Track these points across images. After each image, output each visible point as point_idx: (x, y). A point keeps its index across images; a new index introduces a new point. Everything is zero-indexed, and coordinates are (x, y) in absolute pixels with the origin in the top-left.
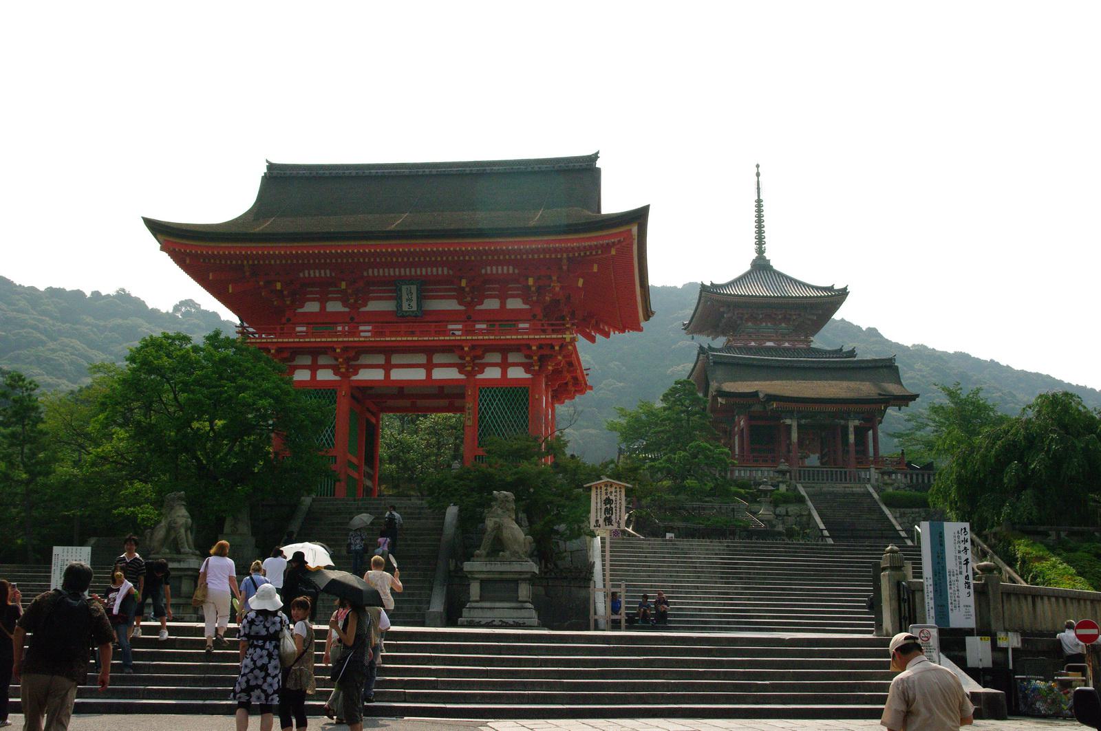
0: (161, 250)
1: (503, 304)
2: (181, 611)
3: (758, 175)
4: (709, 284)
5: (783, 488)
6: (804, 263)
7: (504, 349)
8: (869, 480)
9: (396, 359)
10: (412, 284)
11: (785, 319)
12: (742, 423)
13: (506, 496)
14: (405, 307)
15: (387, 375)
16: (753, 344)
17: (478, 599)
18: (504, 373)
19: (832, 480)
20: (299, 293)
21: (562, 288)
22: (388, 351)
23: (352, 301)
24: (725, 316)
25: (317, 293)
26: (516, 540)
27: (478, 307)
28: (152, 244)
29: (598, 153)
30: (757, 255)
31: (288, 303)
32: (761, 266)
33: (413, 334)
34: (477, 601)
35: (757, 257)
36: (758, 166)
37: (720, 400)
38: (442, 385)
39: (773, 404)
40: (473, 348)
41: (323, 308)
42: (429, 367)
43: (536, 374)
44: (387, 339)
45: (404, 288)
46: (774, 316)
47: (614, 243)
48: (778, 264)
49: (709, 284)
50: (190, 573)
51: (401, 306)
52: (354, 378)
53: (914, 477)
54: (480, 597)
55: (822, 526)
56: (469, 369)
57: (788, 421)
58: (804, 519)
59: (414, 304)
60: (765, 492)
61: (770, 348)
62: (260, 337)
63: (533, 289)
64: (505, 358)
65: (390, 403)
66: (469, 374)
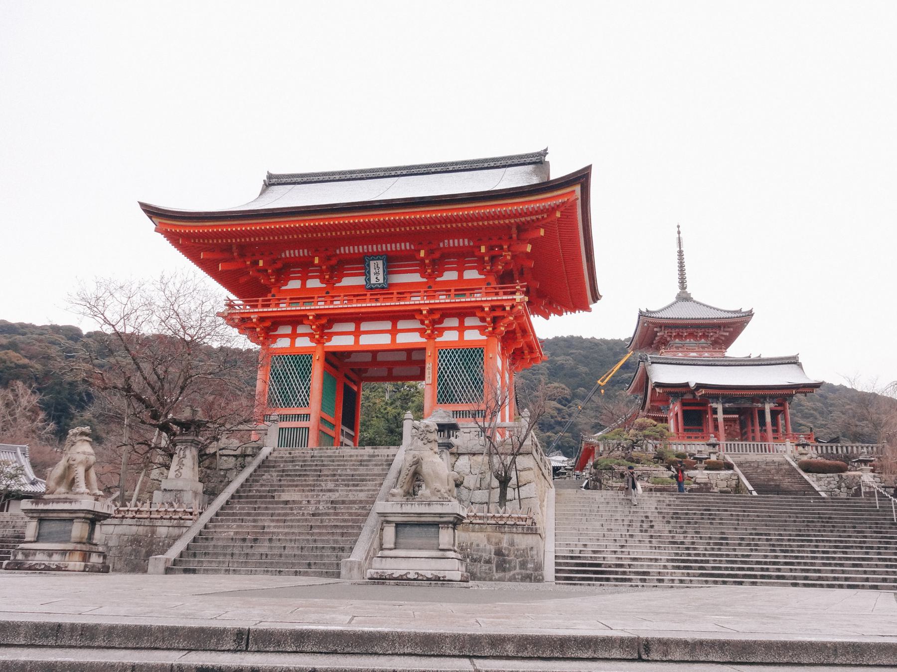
0: (156, 231)
1: (461, 276)
2: (67, 558)
3: (679, 233)
4: (644, 310)
5: (713, 458)
6: (714, 297)
7: (461, 313)
9: (365, 326)
10: (379, 259)
11: (705, 336)
12: (676, 409)
13: (427, 426)
14: (373, 281)
15: (357, 341)
17: (392, 546)
18: (461, 335)
20: (283, 272)
21: (513, 257)
22: (357, 318)
23: (327, 277)
25: (298, 272)
26: (437, 476)
27: (438, 279)
28: (148, 224)
29: (546, 150)
31: (273, 280)
32: (684, 297)
33: (377, 300)
34: (391, 549)
36: (678, 227)
37: (658, 390)
38: (409, 351)
40: (431, 311)
41: (304, 284)
42: (394, 332)
43: (491, 334)
44: (354, 305)
45: (372, 263)
48: (695, 296)
50: (82, 515)
51: (369, 279)
52: (327, 344)
53: (824, 448)
54: (395, 543)
55: (751, 488)
56: (429, 332)
57: (714, 405)
58: (734, 482)
59: (381, 277)
60: (701, 460)
62: (245, 308)
63: (486, 258)
64: (462, 322)
65: (373, 371)
66: (430, 337)
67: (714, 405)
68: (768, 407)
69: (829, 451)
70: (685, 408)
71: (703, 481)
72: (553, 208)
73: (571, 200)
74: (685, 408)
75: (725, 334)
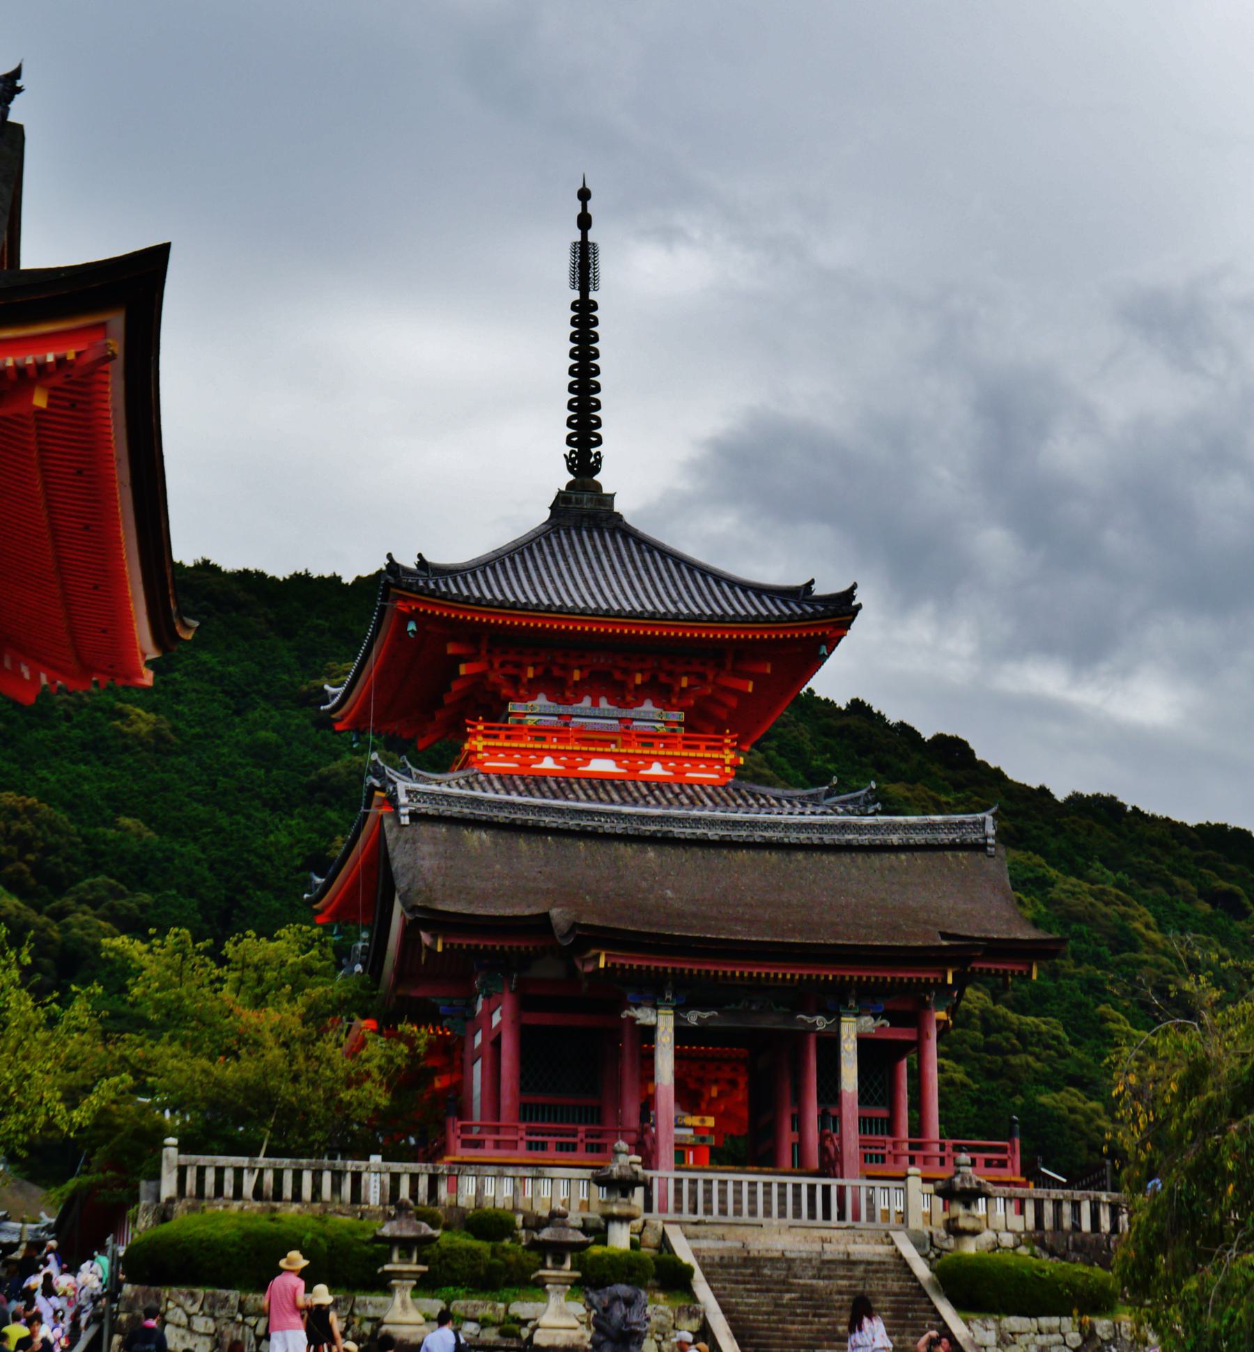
4: (410, 562)
8: (903, 1217)
12: (496, 1018)
16: (548, 763)
19: (782, 1214)
24: (463, 670)
30: (572, 477)
32: (583, 510)
35: (570, 486)
37: (425, 938)
39: (597, 958)
46: (618, 676)
47: (41, 367)
49: (410, 562)
53: (1048, 1208)
57: (644, 1016)
60: (558, 1250)
61: (602, 781)
67: (644, 1016)
68: (850, 1030)
69: (1067, 1223)
70: (532, 1019)
71: (561, 1339)
72: (21, 371)
73: (90, 357)
74: (532, 1019)
75: (736, 684)
